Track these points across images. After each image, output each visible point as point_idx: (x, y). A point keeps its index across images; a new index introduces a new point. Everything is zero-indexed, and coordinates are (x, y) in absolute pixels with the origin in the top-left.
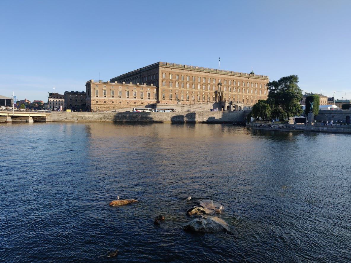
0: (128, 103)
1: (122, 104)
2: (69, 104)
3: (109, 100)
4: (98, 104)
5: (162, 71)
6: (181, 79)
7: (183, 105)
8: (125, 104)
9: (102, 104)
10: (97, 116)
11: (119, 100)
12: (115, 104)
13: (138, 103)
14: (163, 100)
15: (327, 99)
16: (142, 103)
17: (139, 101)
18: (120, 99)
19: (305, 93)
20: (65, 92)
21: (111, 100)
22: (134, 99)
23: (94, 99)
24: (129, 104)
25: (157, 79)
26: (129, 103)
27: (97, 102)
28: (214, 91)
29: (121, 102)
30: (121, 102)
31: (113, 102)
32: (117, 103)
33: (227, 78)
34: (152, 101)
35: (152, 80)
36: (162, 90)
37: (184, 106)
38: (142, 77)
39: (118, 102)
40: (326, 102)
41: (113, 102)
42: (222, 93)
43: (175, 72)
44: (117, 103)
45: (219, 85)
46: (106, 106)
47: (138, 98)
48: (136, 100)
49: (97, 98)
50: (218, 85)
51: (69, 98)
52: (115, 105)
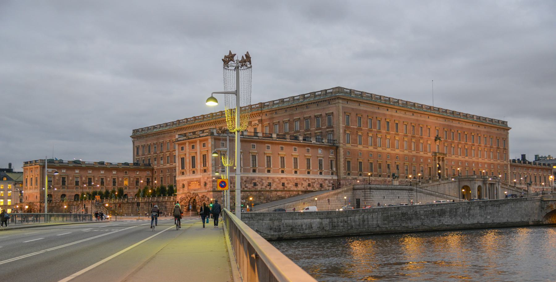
3: (248, 179)
6: (375, 128)
7: (411, 187)
8: (278, 189)
10: (318, 220)
11: (268, 178)
12: (259, 189)
13: (302, 184)
17: (303, 179)
19: (536, 156)
21: (253, 179)
22: (295, 176)
24: (286, 189)
26: (286, 185)
28: (430, 155)
29: (270, 184)
31: (255, 184)
32: (262, 185)
34: (326, 180)
36: (345, 154)
38: (266, 123)
39: (266, 184)
44: (263, 187)
45: (438, 141)
47: (301, 173)
48: (299, 179)
50: (436, 140)
52: (259, 191)
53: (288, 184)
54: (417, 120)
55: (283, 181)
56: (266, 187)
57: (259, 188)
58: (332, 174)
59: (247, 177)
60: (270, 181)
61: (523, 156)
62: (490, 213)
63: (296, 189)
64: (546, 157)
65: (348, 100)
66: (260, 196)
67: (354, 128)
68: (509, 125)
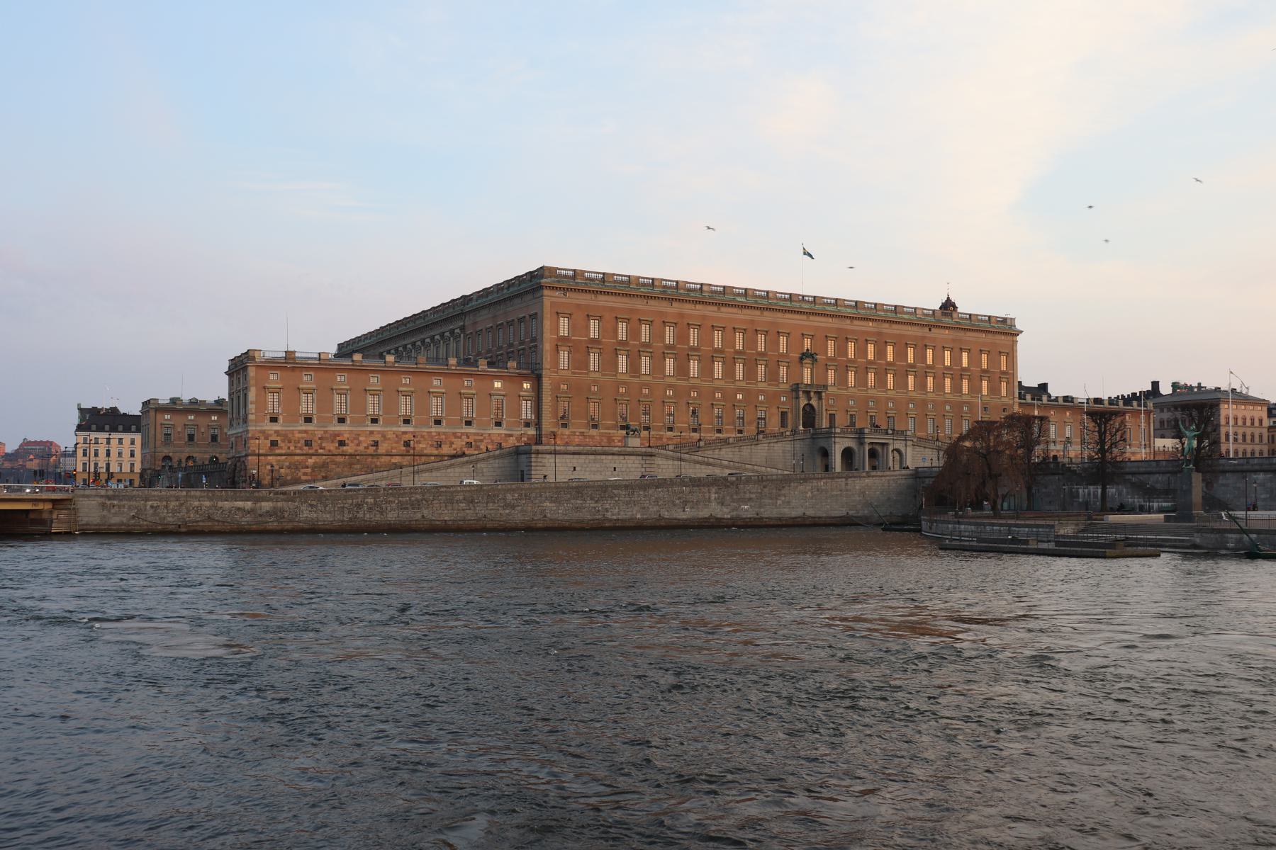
0: (407, 444)
1: (382, 450)
2: (161, 455)
4: (278, 451)
5: (552, 303)
9: (298, 451)
11: (372, 432)
13: (452, 443)
14: (561, 430)
15: (1265, 409)
16: (469, 445)
17: (454, 434)
18: (375, 428)
19: (1175, 386)
20: (146, 404)
22: (434, 429)
23: (263, 432)
25: (534, 340)
27: (274, 444)
29: (376, 444)
30: (376, 444)
31: (342, 443)
32: (358, 445)
33: (839, 330)
34: (511, 435)
35: (511, 345)
36: (556, 388)
37: (652, 455)
39: (365, 441)
40: (1261, 421)
41: (342, 443)
42: (819, 394)
43: (612, 309)
45: (807, 361)
46: (311, 461)
49: (276, 427)
51: (158, 427)
53: (419, 442)
54: (752, 322)
55: (406, 437)
56: (367, 448)
57: (349, 449)
58: (527, 425)
59: (326, 432)
60: (377, 437)
61: (1155, 385)
62: (750, 499)
63: (436, 452)
64: (1191, 388)
65: (565, 290)
66: (351, 465)
67: (580, 341)
68: (1019, 327)
